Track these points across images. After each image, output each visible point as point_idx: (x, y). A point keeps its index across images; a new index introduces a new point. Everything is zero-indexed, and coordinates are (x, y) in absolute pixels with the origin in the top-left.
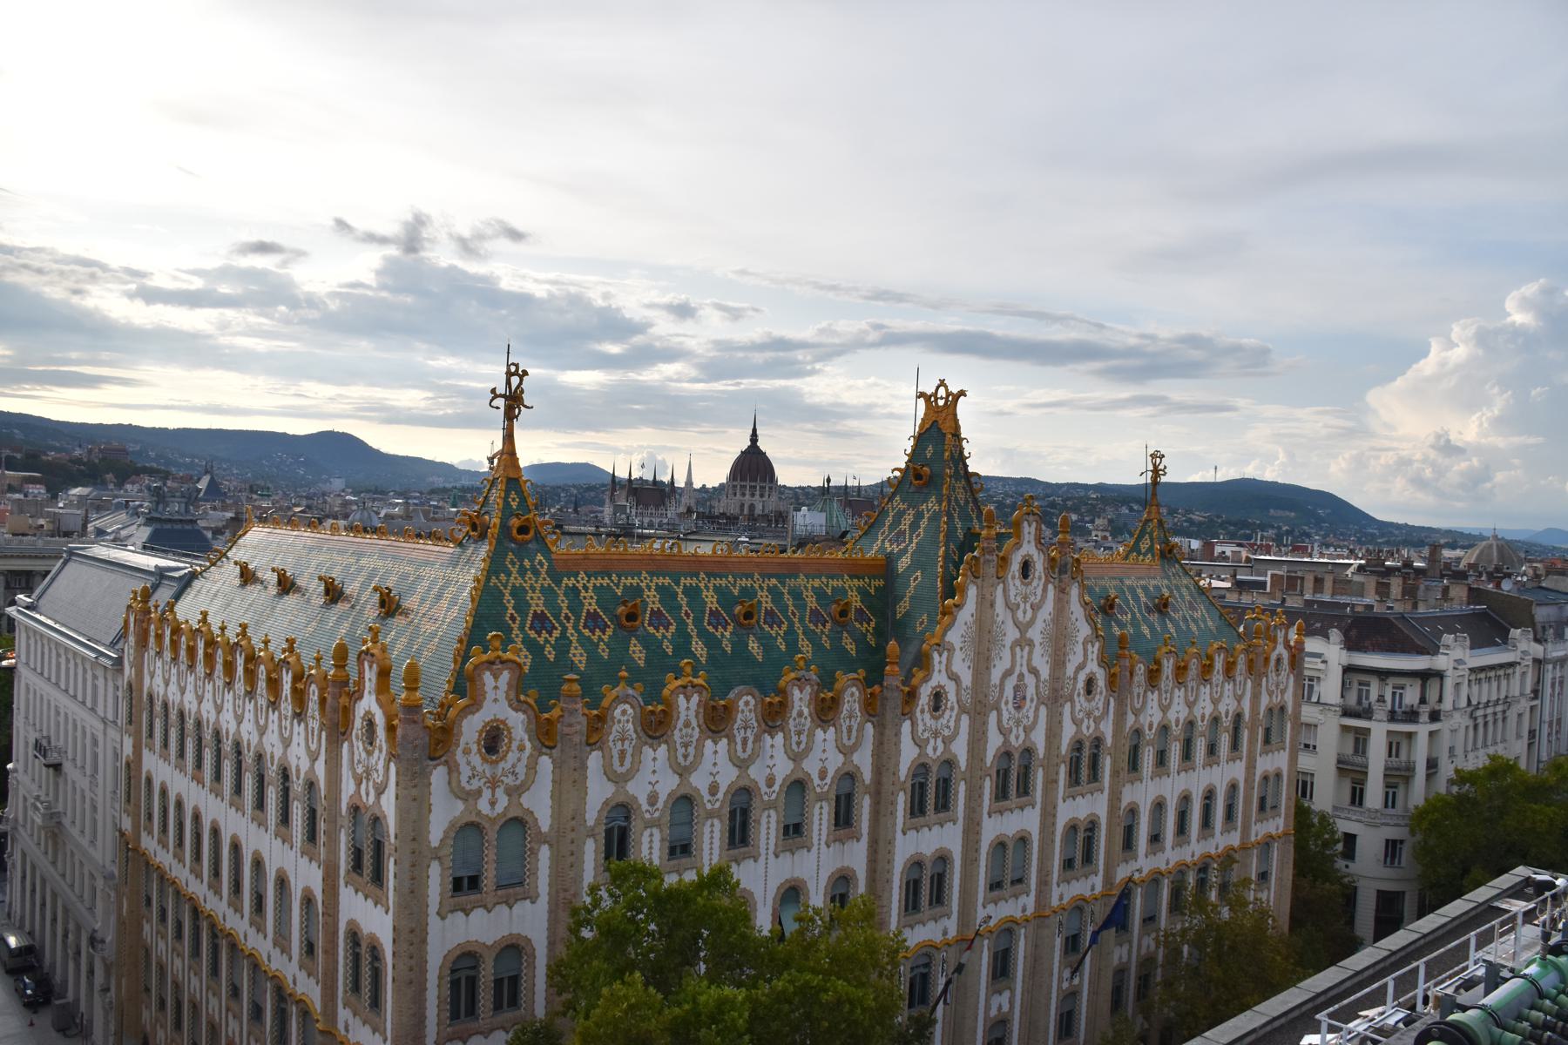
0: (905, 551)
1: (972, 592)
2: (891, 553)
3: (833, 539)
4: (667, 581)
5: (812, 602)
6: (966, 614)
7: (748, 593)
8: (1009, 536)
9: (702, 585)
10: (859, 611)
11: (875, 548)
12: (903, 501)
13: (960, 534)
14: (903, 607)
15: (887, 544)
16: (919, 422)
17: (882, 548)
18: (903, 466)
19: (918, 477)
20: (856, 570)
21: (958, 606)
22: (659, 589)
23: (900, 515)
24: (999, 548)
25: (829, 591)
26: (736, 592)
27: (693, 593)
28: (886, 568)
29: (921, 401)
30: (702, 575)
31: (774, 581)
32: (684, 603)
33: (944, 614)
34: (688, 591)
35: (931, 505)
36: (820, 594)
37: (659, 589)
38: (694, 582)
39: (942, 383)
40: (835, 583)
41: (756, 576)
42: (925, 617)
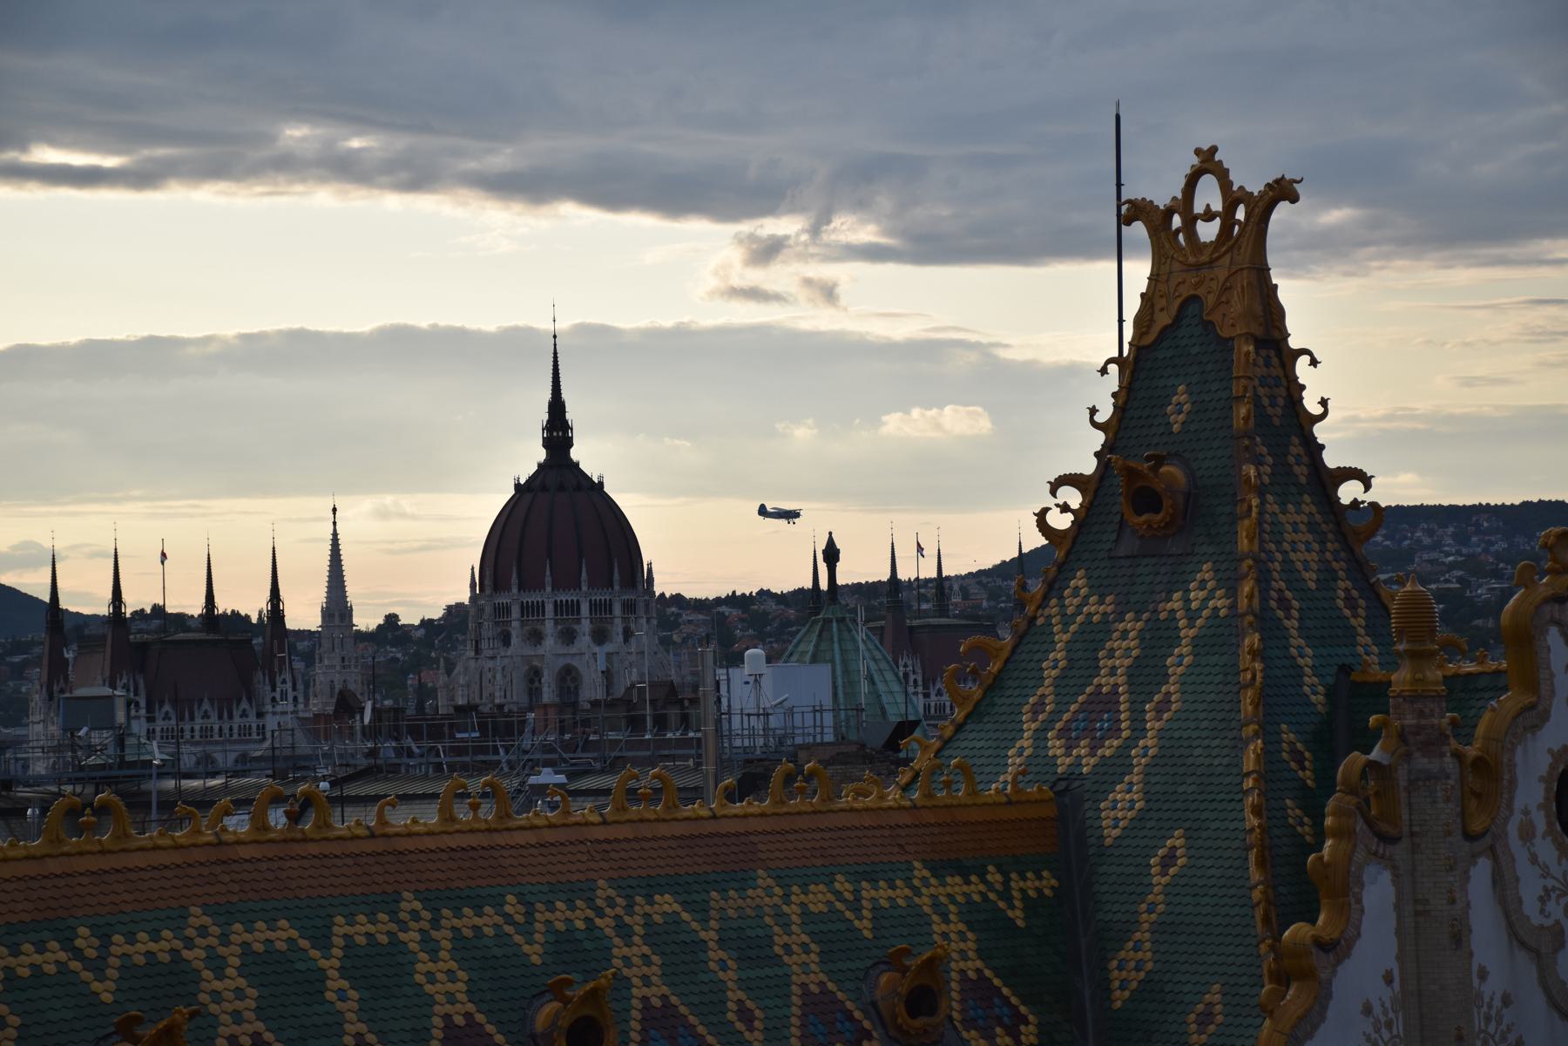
0: (1117, 768)
1: (1378, 893)
2: (1072, 776)
3: (863, 755)
4: (284, 932)
5: (806, 969)
6: (1369, 969)
7: (573, 950)
8: (1495, 684)
9: (411, 938)
10: (978, 989)
11: (1014, 761)
12: (1099, 588)
13: (1314, 690)
14: (1131, 965)
15: (1055, 747)
16: (1132, 306)
17: (1039, 762)
18: (1088, 466)
19: (1145, 499)
20: (958, 842)
21: (1335, 948)
22: (260, 965)
23: (1092, 638)
24: (1462, 730)
25: (865, 926)
26: (534, 953)
27: (380, 971)
28: (1056, 826)
29: (1138, 230)
30: (410, 903)
31: (667, 903)
32: (349, 1007)
33: (1282, 979)
34: (358, 964)
35: (1200, 596)
36: (832, 938)
37: (260, 965)
38: (382, 928)
39: (1207, 163)
40: (883, 893)
41: (604, 890)
42: (1214, 996)
